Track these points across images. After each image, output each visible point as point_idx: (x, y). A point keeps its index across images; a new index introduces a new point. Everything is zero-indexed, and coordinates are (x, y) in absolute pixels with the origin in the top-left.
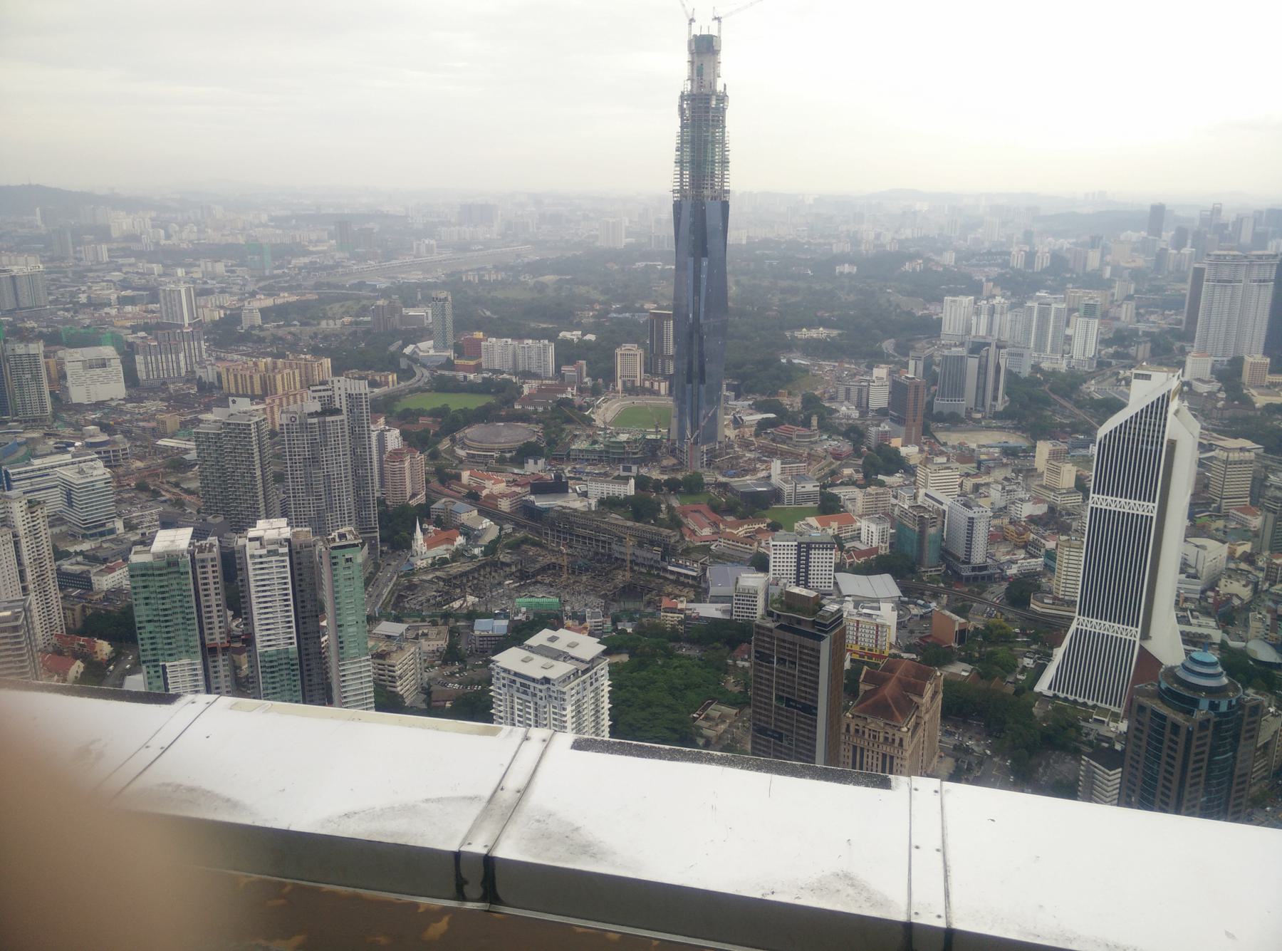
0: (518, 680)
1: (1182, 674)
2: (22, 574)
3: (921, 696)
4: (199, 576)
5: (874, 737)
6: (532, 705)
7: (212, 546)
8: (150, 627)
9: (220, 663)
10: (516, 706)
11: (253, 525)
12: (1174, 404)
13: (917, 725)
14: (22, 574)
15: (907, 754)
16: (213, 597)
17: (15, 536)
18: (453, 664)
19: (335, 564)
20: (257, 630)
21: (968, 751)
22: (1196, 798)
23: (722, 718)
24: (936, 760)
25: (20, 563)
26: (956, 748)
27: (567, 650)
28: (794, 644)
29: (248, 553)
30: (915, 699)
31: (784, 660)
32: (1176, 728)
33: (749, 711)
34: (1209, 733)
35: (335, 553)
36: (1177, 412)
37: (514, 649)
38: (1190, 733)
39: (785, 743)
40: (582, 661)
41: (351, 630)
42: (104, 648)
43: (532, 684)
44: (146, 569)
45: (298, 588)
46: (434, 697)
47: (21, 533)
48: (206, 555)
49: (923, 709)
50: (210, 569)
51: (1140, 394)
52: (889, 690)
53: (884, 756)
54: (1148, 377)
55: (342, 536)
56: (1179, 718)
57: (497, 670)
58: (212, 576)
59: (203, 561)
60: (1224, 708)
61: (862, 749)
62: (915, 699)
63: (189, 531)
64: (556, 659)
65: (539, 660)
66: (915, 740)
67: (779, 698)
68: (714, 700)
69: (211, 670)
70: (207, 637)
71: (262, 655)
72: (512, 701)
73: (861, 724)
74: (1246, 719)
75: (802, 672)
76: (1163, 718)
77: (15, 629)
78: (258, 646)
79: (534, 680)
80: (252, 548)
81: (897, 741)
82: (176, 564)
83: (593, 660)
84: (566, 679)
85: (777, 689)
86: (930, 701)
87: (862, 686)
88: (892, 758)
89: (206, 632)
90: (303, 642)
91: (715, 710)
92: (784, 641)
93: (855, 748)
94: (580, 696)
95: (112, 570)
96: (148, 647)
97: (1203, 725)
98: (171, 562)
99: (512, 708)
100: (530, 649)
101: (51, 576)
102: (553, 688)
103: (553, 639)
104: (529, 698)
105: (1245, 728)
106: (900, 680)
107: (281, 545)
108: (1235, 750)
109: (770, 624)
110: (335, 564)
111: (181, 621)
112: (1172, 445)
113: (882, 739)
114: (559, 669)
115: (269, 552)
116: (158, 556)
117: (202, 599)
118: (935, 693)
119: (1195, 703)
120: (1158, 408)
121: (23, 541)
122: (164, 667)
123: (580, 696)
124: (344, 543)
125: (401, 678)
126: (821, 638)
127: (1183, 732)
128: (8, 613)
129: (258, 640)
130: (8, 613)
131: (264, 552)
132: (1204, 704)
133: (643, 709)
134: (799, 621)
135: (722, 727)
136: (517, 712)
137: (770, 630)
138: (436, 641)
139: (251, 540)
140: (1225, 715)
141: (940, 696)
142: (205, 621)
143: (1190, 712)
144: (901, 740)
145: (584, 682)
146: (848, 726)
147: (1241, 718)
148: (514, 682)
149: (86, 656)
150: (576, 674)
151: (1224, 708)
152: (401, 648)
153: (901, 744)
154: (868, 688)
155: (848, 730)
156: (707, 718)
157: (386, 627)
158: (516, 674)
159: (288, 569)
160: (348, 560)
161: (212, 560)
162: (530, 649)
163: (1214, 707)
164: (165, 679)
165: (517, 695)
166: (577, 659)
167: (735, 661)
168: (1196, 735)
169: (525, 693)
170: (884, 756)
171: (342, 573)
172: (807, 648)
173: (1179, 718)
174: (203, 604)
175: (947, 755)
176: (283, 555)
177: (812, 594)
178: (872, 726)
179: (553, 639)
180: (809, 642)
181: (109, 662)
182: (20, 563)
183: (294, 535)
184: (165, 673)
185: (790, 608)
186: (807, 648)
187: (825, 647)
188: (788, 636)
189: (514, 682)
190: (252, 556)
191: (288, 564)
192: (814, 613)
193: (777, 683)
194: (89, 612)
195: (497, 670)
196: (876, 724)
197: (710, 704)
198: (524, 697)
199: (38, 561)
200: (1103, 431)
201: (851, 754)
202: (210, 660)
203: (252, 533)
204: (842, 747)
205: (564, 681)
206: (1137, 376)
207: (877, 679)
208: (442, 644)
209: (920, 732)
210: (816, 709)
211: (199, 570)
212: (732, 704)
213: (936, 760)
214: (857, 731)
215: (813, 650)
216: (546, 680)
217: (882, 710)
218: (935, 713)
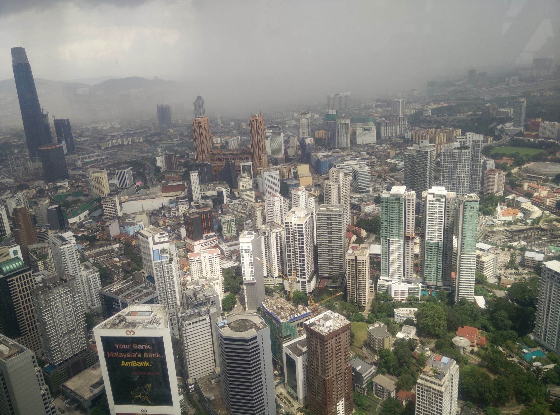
2: (339, 199)
4: (407, 206)
7: (413, 195)
8: (386, 223)
9: (410, 243)
10: (553, 289)
11: (430, 188)
14: (339, 199)
16: (411, 215)
17: (339, 186)
18: (511, 269)
19: (466, 208)
20: (427, 232)
25: (339, 196)
29: (428, 199)
35: (466, 204)
37: (555, 261)
42: (364, 233)
44: (388, 200)
45: (446, 218)
46: (501, 282)
47: (341, 185)
48: (410, 197)
50: (411, 204)
55: (469, 197)
57: (545, 269)
58: (412, 208)
59: (409, 200)
63: (405, 187)
69: (406, 245)
70: (407, 231)
71: (428, 243)
72: (551, 286)
77: (340, 215)
78: (427, 239)
80: (430, 197)
82: (399, 200)
89: (407, 229)
90: (445, 241)
95: (367, 205)
96: (384, 231)
98: (397, 197)
99: (551, 289)
101: (348, 202)
107: (442, 198)
110: (466, 208)
111: (397, 223)
115: (436, 200)
116: (392, 195)
117: (407, 215)
121: (341, 188)
122: (389, 240)
124: (471, 200)
128: (338, 209)
129: (427, 237)
130: (338, 209)
131: (434, 199)
136: (553, 292)
138: (505, 257)
139: (430, 194)
142: (407, 225)
148: (554, 276)
149: (358, 234)
152: (488, 255)
157: (481, 245)
158: (556, 273)
159: (444, 208)
160: (472, 208)
161: (413, 200)
164: (389, 245)
165: (554, 283)
171: (468, 213)
174: (407, 218)
176: (442, 202)
181: (366, 238)
182: (339, 196)
183: (448, 195)
184: (389, 243)
189: (554, 276)
190: (430, 201)
191: (444, 206)
194: (359, 219)
199: (345, 197)
202: (407, 243)
203: (430, 191)
208: (508, 259)
211: (407, 203)
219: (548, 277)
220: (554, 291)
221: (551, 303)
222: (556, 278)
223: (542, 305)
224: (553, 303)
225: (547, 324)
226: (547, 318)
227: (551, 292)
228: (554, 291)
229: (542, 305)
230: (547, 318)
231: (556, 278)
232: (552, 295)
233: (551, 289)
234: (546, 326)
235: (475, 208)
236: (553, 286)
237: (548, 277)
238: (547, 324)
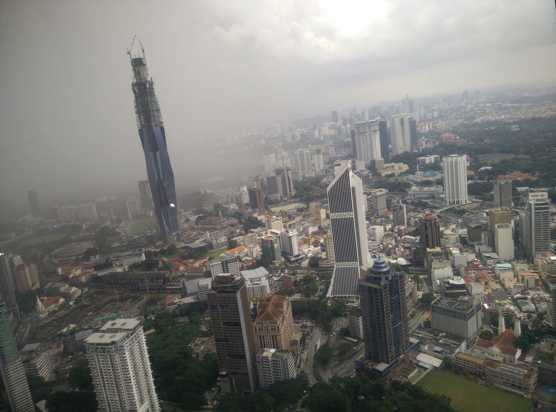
0: (99, 347)
1: (374, 270)
3: (282, 307)
5: (267, 329)
6: (108, 357)
10: (101, 360)
12: (351, 173)
13: (283, 320)
15: (282, 333)
21: (305, 327)
22: (389, 316)
23: (203, 343)
24: (294, 334)
26: (302, 327)
27: (121, 327)
28: (225, 298)
30: (280, 309)
31: (223, 306)
32: (376, 290)
33: (213, 337)
34: (387, 289)
36: (352, 176)
39: (230, 342)
40: (130, 330)
41: (7, 348)
43: (106, 347)
49: (285, 313)
51: (338, 172)
52: (270, 308)
53: (273, 336)
54: (340, 165)
56: (376, 286)
57: (87, 345)
60: (390, 278)
61: (263, 336)
62: (280, 309)
64: (117, 332)
65: (108, 335)
66: (284, 327)
67: (224, 323)
68: (197, 336)
72: (98, 358)
73: (260, 326)
74: (399, 281)
76: (371, 288)
79: (107, 344)
81: (276, 328)
83: (135, 328)
84: (123, 339)
85: (222, 320)
86: (287, 310)
87: (258, 311)
88: (276, 336)
91: (198, 341)
92: (221, 298)
93: (260, 337)
94: (131, 346)
99: (99, 361)
100: (103, 331)
102: (117, 346)
103: (113, 324)
104: (106, 354)
105: (399, 284)
106: (273, 304)
108: (398, 294)
109: (213, 292)
112: (354, 188)
113: (270, 330)
114: (118, 336)
118: (288, 305)
119: (380, 279)
123: (131, 346)
125: (40, 368)
126: (235, 292)
127: (379, 291)
133: (165, 348)
134: (226, 288)
135: (202, 347)
136: (101, 363)
137: (214, 295)
140: (390, 281)
141: (290, 307)
143: (379, 283)
144: (278, 327)
145: (132, 339)
146: (256, 328)
147: (397, 280)
148: (97, 348)
150: (128, 337)
151: (390, 278)
153: (278, 329)
154: (261, 310)
155: (256, 330)
156: (196, 345)
158: (98, 344)
162: (103, 331)
163: (387, 279)
165: (99, 354)
166: (127, 330)
167: (204, 318)
168: (383, 291)
169: (104, 352)
170: (273, 336)
172: (231, 298)
173: (376, 286)
175: (298, 331)
177: (229, 274)
178: (265, 325)
179: (113, 324)
180: (231, 295)
185: (220, 283)
186: (231, 298)
187: (238, 295)
188: (222, 295)
189: (97, 348)
192: (231, 282)
193: (222, 317)
195: (87, 345)
196: (267, 323)
197: (195, 339)
198: (104, 354)
200: (328, 189)
201: (259, 340)
204: (255, 338)
205: (122, 341)
206: (336, 165)
207: (264, 306)
208: (61, 349)
209: (285, 322)
210: (240, 323)
212: (205, 336)
213: (294, 334)
214: (260, 329)
216: (113, 343)
217: (269, 317)
218: (289, 315)
219: (93, 352)
220: (102, 361)
221: (104, 374)
222: (100, 349)
223: (97, 380)
224: (105, 372)
225: (107, 395)
226: (105, 389)
227: (99, 364)
228: (102, 361)
229: (97, 380)
230: (105, 389)
231: (100, 349)
232: (102, 366)
233: (99, 361)
234: (107, 398)
235: (3, 313)
236: (100, 357)
237: (93, 352)
238: (107, 395)
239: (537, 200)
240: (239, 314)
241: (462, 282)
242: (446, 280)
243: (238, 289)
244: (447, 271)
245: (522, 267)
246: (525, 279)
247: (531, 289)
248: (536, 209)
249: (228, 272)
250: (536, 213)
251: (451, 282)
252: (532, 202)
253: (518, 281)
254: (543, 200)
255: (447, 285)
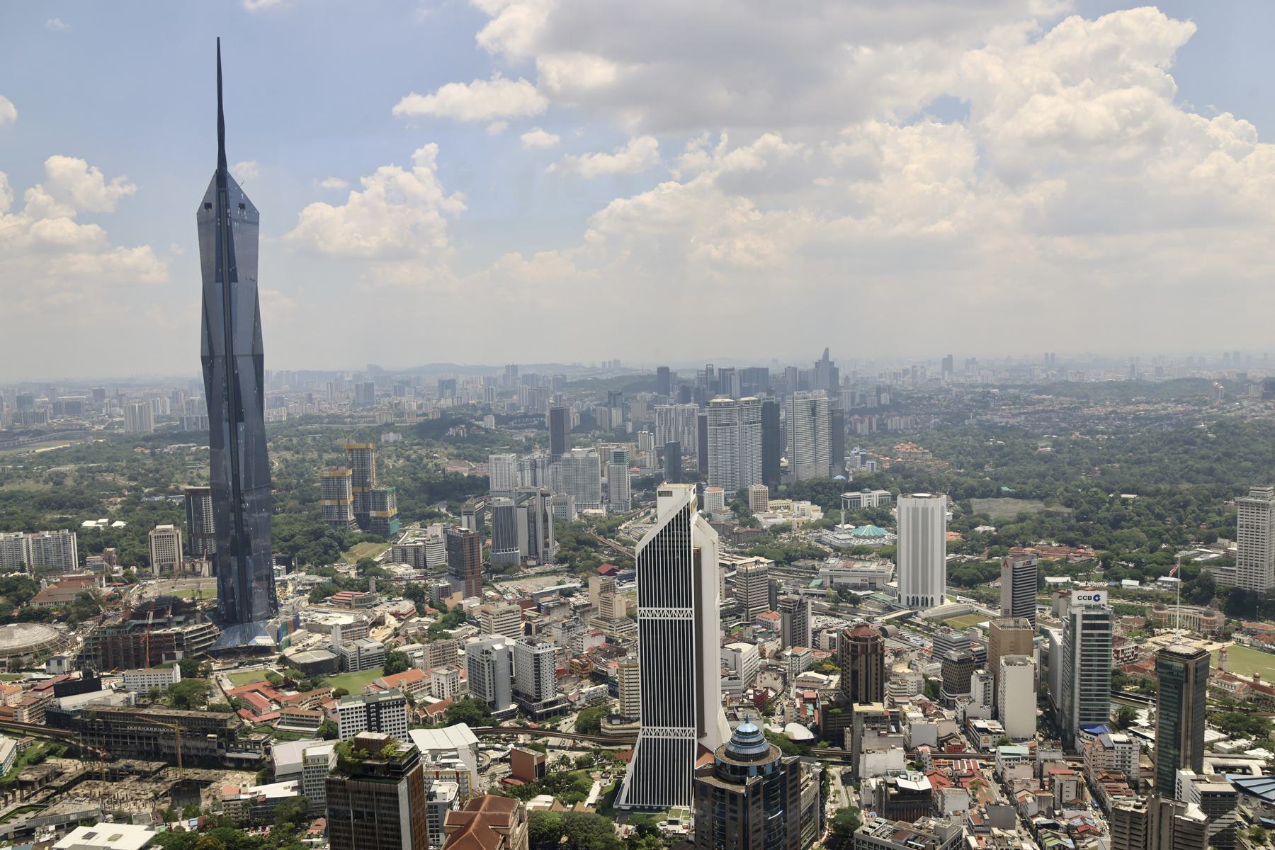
1: (732, 749)
12: (695, 517)
28: (370, 793)
32: (734, 796)
34: (761, 796)
38: (744, 798)
51: (666, 509)
54: (669, 494)
60: (769, 771)
74: (789, 778)
75: (383, 822)
76: (723, 791)
97: (756, 786)
103: (89, 836)
105: (789, 786)
112: (698, 553)
120: (682, 520)
132: (753, 771)
141: (524, 826)
143: (742, 782)
151: (769, 771)
179: (89, 836)
180: (385, 786)
193: (357, 840)
206: (662, 494)
215: (391, 795)
239: (1088, 607)
240: (400, 837)
241: (925, 784)
242: (890, 780)
243: (403, 774)
244: (895, 758)
245: (1053, 756)
246: (1057, 782)
247: (1068, 805)
248: (1085, 627)
249: (380, 731)
250: (1083, 635)
251: (903, 783)
252: (1078, 612)
253: (1042, 786)
254: (1098, 607)
255: (893, 791)
